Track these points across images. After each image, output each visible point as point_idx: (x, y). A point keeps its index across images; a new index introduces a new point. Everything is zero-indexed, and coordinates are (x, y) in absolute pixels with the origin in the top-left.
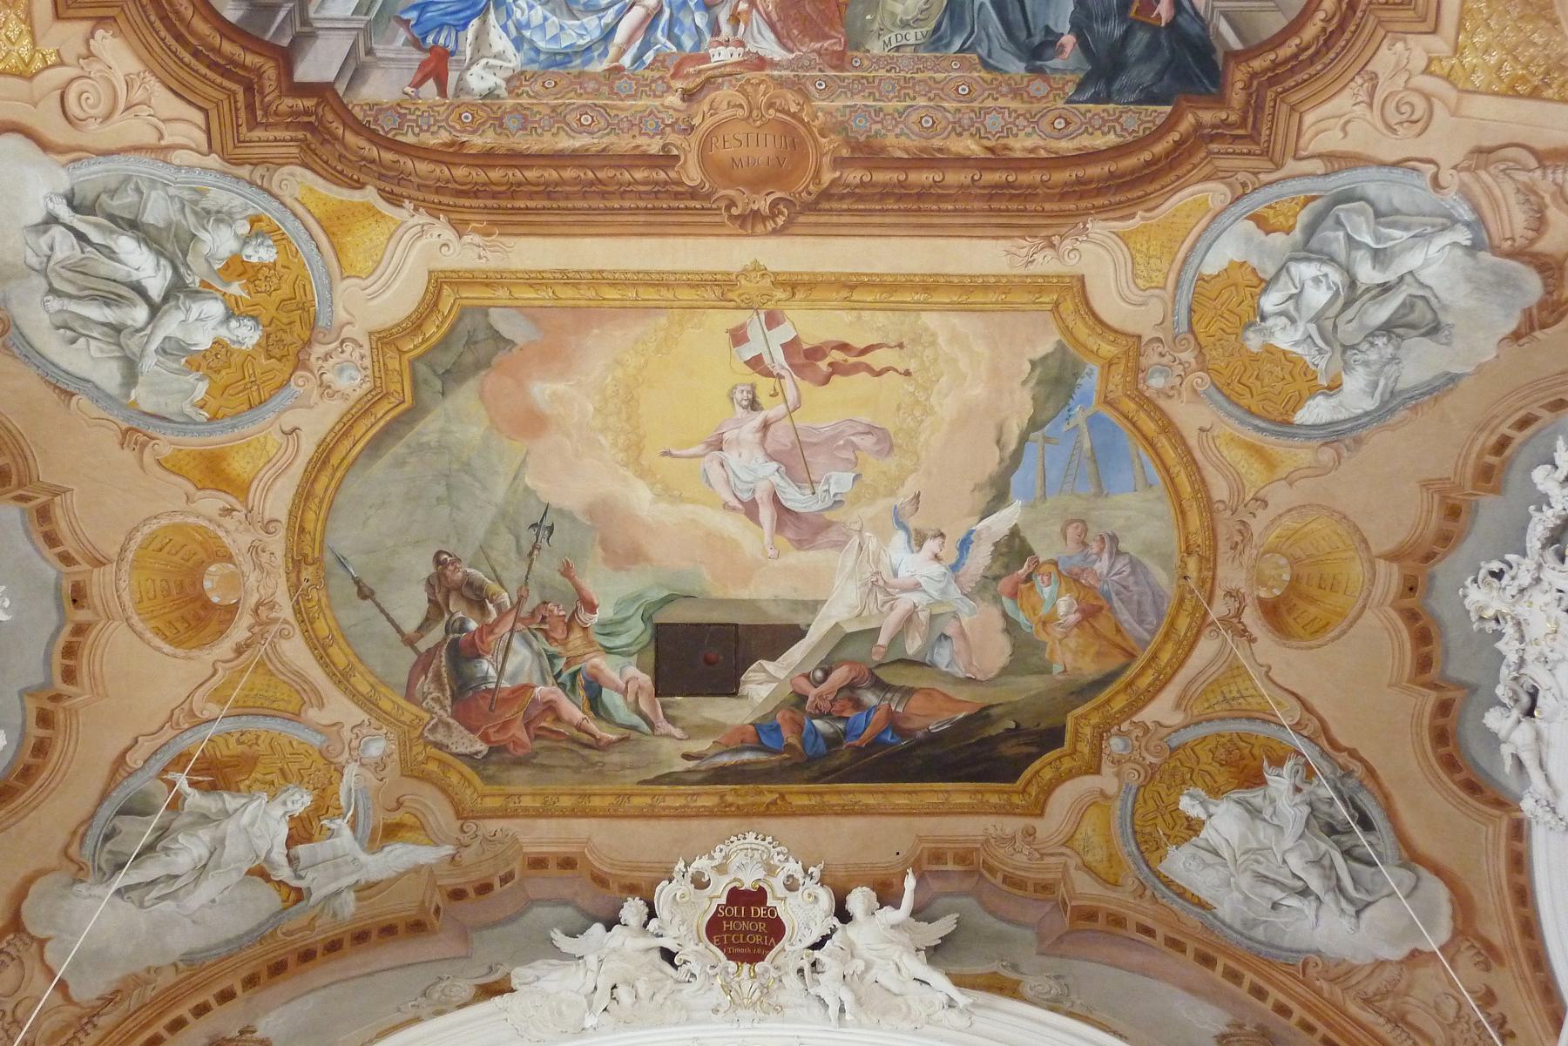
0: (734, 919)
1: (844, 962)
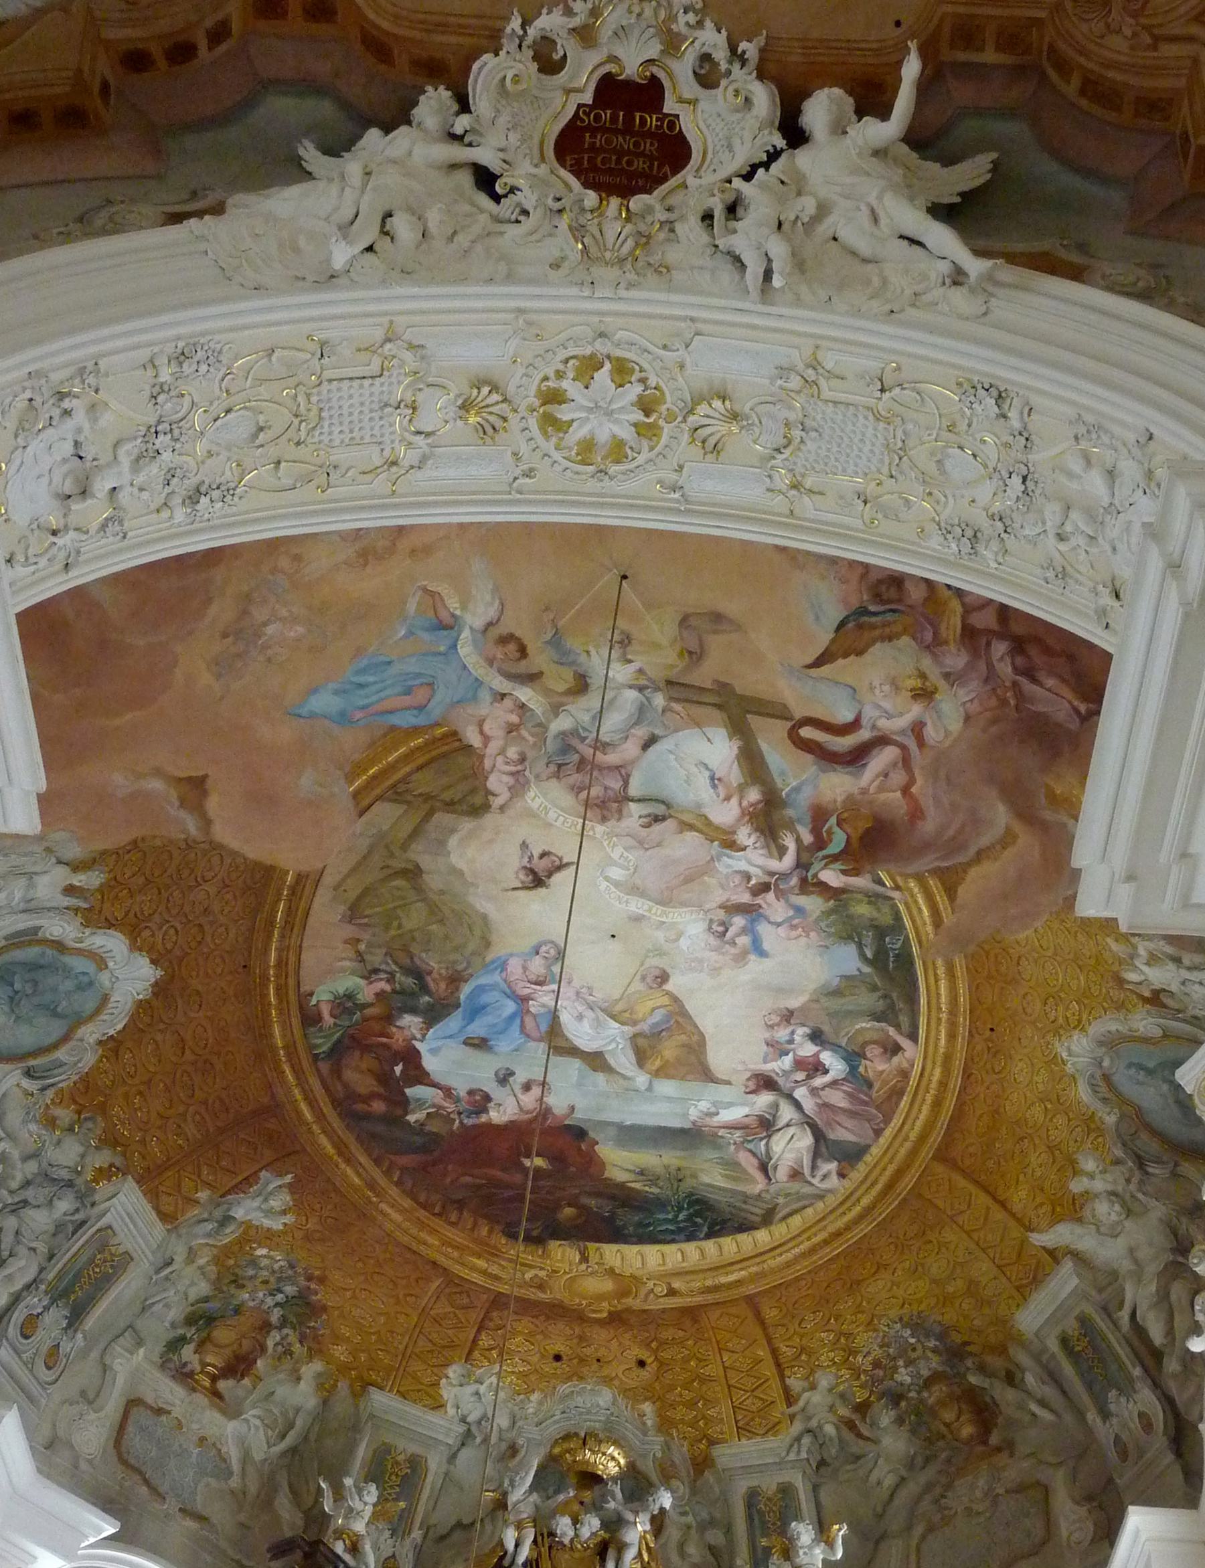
0: (604, 130)
1: (782, 200)
